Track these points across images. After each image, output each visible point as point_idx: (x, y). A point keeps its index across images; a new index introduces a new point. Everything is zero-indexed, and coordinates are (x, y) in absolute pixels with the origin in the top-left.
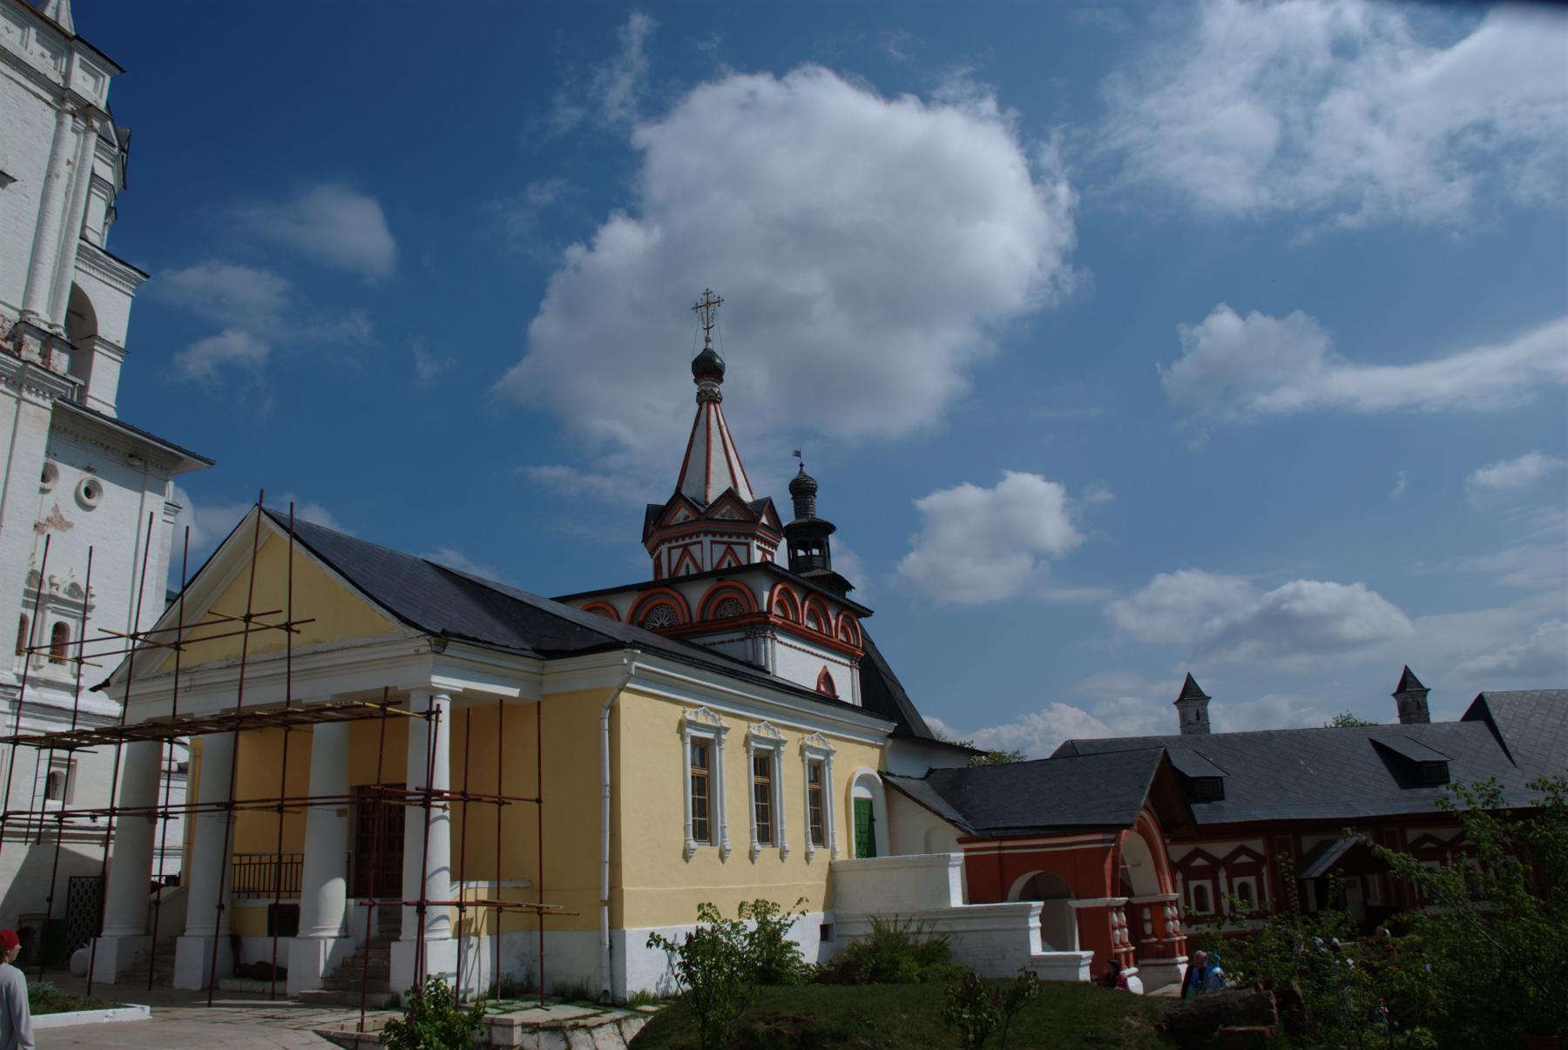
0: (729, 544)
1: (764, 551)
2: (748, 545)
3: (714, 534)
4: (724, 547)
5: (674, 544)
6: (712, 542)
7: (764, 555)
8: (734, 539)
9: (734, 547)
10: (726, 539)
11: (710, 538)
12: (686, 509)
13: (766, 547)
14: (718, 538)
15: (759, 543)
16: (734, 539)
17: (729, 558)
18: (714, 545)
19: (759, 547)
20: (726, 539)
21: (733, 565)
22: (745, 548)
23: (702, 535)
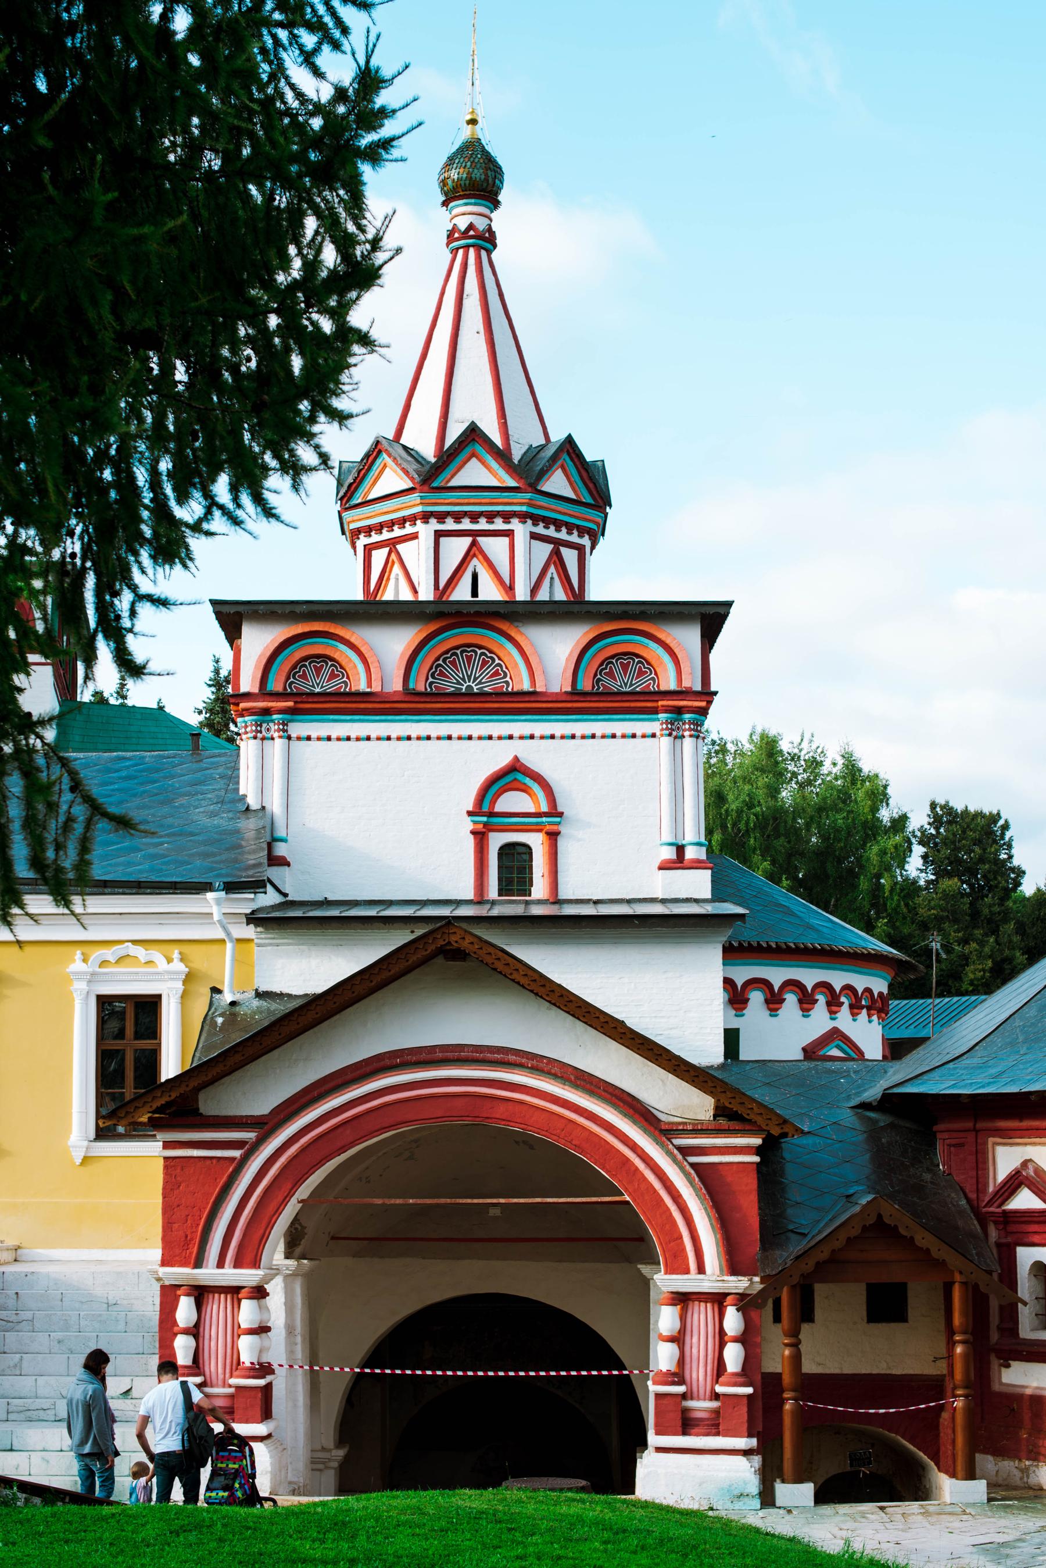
0: (474, 534)
2: (509, 534)
3: (441, 517)
4: (468, 540)
5: (375, 538)
6: (439, 534)
8: (483, 525)
9: (481, 540)
10: (466, 525)
11: (434, 525)
14: (450, 525)
16: (483, 525)
17: (475, 562)
18: (443, 540)
19: (534, 536)
20: (466, 525)
22: (506, 540)
23: (418, 522)
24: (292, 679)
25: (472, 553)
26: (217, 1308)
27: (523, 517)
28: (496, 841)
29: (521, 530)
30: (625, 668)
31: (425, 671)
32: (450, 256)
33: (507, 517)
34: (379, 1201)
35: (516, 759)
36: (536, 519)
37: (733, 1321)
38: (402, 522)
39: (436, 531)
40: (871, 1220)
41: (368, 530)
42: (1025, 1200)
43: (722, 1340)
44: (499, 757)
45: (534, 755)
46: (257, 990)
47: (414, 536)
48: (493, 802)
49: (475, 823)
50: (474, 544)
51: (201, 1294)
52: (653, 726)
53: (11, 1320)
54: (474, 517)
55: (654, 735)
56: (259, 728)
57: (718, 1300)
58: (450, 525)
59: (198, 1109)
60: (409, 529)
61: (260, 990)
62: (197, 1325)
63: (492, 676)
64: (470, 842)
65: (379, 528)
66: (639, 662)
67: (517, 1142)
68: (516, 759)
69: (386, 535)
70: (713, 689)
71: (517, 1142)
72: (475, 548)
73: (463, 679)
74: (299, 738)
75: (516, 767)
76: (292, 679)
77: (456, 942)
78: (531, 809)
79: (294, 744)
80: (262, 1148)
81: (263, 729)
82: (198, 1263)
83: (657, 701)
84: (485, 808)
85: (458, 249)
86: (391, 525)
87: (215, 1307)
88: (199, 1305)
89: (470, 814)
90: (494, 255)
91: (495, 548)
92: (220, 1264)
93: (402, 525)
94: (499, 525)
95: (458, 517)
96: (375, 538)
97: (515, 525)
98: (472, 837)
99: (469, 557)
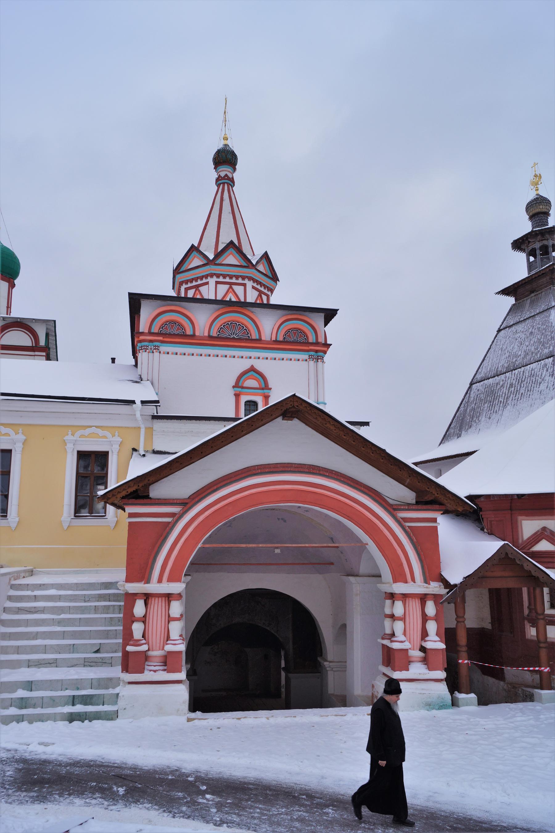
0: (231, 284)
1: (261, 292)
2: (244, 285)
3: (218, 276)
4: (227, 287)
5: (190, 285)
6: (217, 283)
7: (260, 296)
8: (234, 280)
9: (234, 287)
10: (227, 280)
11: (215, 279)
12: (199, 259)
13: (262, 289)
14: (221, 279)
15: (255, 285)
16: (234, 280)
18: (218, 285)
19: (253, 287)
20: (227, 280)
21: (234, 299)
22: (242, 287)
23: (209, 278)
24: (161, 329)
25: (230, 291)
26: (157, 606)
27: (250, 279)
28: (244, 399)
29: (249, 284)
30: (295, 334)
31: (224, 321)
32: (217, 188)
33: (243, 278)
34: (244, 545)
35: (252, 366)
36: (255, 281)
37: (431, 609)
38: (201, 278)
39: (216, 281)
40: (503, 556)
41: (186, 282)
42: (544, 546)
43: (425, 618)
44: (245, 365)
45: (260, 365)
46: (154, 450)
47: (207, 283)
48: (243, 383)
49: (235, 391)
50: (231, 287)
51: (147, 597)
52: (306, 357)
53: (31, 611)
54: (231, 277)
55: (306, 360)
56: (147, 348)
57: (423, 598)
58: (221, 279)
59: (149, 496)
60: (204, 281)
61: (155, 450)
62: (145, 616)
63: (242, 334)
64: (233, 399)
65: (191, 281)
66: (300, 332)
67: (279, 519)
68: (252, 366)
69: (194, 283)
70: (328, 342)
71: (279, 519)
72: (231, 290)
73: (231, 334)
74: (164, 353)
75: (252, 369)
76: (161, 329)
77: (297, 406)
78: (258, 386)
79: (162, 355)
80: (184, 516)
81: (149, 348)
82: (148, 581)
83: (309, 346)
84: (240, 384)
85: (220, 184)
86: (196, 279)
87: (156, 606)
88: (146, 604)
89: (234, 387)
90: (234, 188)
91: (239, 290)
92: (160, 581)
93: (202, 279)
94: (240, 281)
95: (224, 276)
96: (190, 285)
97: (246, 281)
98: (234, 397)
99: (228, 293)
